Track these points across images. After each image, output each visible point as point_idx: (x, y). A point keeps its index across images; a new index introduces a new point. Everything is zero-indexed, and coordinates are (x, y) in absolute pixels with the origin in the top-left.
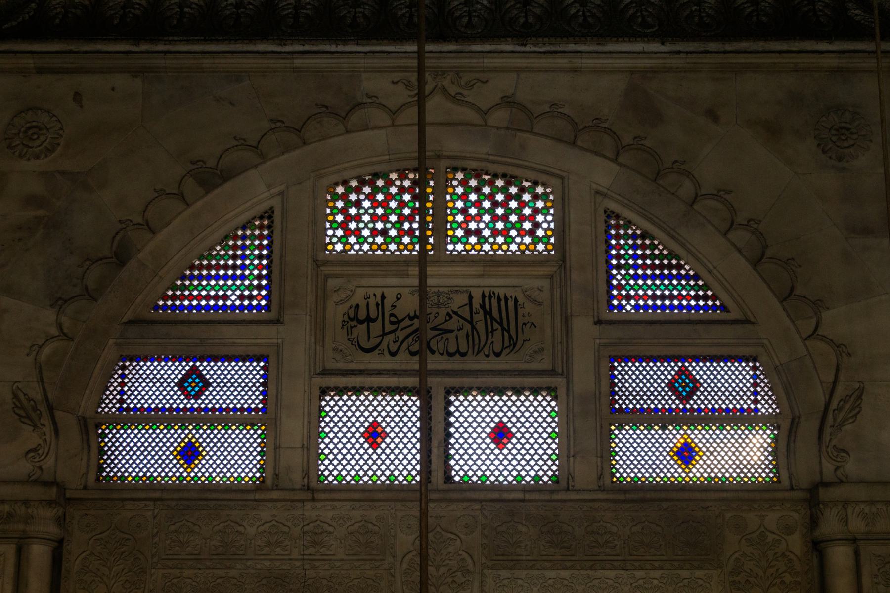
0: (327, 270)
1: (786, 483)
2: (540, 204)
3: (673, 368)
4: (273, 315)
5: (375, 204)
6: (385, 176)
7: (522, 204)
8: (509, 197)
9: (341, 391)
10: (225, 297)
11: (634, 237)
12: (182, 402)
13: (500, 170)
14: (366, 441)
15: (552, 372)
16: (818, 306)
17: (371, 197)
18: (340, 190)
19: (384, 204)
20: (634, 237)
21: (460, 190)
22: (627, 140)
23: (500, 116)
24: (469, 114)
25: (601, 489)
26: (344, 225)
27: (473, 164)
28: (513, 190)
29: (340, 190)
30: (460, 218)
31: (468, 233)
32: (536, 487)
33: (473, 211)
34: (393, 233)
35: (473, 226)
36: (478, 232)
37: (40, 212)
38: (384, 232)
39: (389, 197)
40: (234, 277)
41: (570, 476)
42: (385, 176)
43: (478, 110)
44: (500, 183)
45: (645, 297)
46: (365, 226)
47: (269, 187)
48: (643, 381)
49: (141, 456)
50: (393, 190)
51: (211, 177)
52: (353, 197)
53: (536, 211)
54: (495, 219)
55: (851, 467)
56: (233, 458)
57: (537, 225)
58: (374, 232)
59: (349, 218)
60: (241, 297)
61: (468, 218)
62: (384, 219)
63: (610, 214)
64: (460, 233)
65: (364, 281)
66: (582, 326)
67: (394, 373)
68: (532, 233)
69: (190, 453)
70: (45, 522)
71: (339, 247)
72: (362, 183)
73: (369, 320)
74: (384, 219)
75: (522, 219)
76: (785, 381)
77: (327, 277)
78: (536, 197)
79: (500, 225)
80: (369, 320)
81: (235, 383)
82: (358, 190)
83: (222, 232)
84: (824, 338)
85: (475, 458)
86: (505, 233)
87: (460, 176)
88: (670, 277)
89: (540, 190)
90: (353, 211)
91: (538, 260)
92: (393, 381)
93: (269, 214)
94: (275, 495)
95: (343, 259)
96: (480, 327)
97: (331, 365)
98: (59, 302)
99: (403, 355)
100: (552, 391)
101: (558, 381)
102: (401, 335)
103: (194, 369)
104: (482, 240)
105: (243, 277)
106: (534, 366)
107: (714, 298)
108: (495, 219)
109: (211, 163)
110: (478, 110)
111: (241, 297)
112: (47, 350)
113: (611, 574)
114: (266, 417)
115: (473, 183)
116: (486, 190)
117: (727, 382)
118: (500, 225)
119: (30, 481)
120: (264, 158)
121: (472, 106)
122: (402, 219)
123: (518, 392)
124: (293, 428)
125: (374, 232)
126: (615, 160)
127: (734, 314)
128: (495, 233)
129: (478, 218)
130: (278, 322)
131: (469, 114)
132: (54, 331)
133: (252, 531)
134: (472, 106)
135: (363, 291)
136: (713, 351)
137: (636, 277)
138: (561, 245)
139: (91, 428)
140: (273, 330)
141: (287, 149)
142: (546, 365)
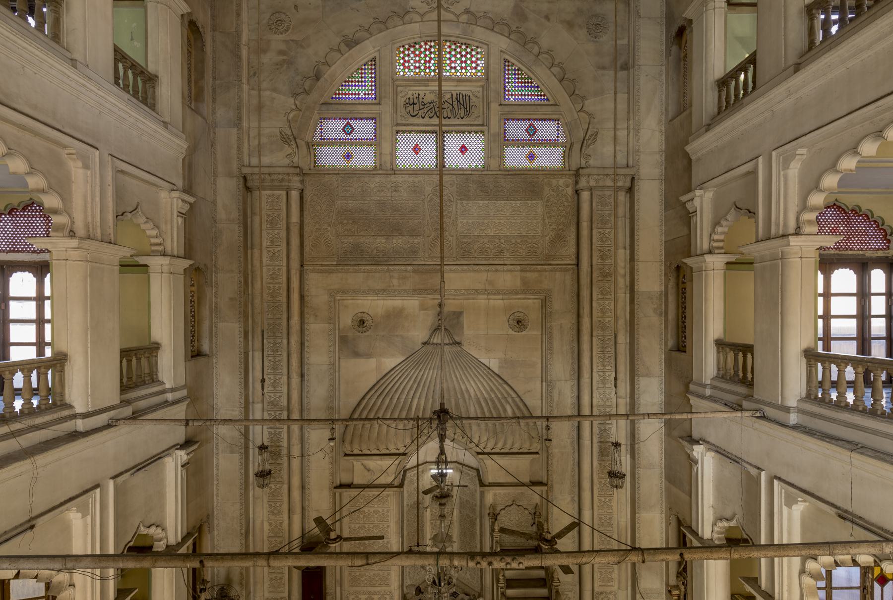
0: (397, 83)
1: (567, 168)
2: (479, 56)
3: (528, 123)
4: (377, 101)
5: (416, 56)
6: (419, 43)
7: (472, 56)
8: (467, 53)
9: (404, 132)
10: (359, 94)
11: (515, 70)
12: (344, 136)
13: (464, 41)
14: (415, 152)
15: (483, 125)
16: (583, 98)
17: (413, 52)
18: (402, 49)
19: (419, 56)
20: (515, 70)
21: (448, 50)
22: (514, 28)
23: (464, 18)
24: (452, 17)
25: (500, 170)
26: (403, 64)
27: (453, 39)
28: (469, 50)
29: (402, 49)
30: (448, 62)
31: (451, 68)
32: (476, 169)
33: (453, 59)
34: (422, 68)
35: (453, 65)
36: (455, 68)
37: (285, 57)
38: (419, 67)
39: (421, 53)
40: (362, 86)
41: (489, 165)
42: (419, 43)
43: (456, 15)
44: (464, 47)
45: (518, 95)
46: (412, 67)
47: (374, 48)
48: (517, 129)
49: (331, 158)
50: (422, 50)
51: (352, 43)
52: (407, 52)
53: (477, 59)
54: (462, 62)
55: (592, 162)
56: (364, 159)
57: (478, 65)
58: (415, 67)
59: (405, 61)
60: (365, 94)
61: (452, 62)
62: (419, 62)
63: (506, 61)
64: (448, 68)
65: (412, 88)
66: (494, 106)
67: (424, 125)
68: (476, 68)
69: (348, 156)
70: (296, 182)
71: (402, 74)
72: (410, 46)
73: (414, 104)
74: (419, 62)
75: (472, 62)
76: (570, 129)
77: (398, 86)
78: (477, 53)
79: (463, 65)
80: (414, 104)
81: (364, 129)
82: (409, 49)
83: (356, 67)
84: (585, 112)
85: (454, 159)
86: (465, 68)
87: (448, 44)
88: (528, 87)
89: (479, 50)
90: (407, 58)
91: (477, 80)
92: (423, 128)
93: (374, 59)
94: (380, 172)
95: (404, 79)
96: (456, 107)
97: (400, 122)
98: (295, 95)
99: (427, 118)
100: (482, 132)
101: (485, 128)
102: (426, 110)
103: (348, 123)
104: (457, 71)
105: (365, 86)
106: (476, 123)
107: (544, 95)
108: (462, 62)
109: (351, 37)
110: (456, 15)
111: (365, 94)
112: (291, 115)
113: (503, 202)
114: (376, 142)
115: (453, 47)
116: (458, 50)
117: (547, 130)
118: (463, 65)
119: (288, 166)
120: (371, 35)
121: (453, 13)
122: (426, 62)
123: (470, 133)
124: (386, 147)
125: (415, 67)
126: (508, 37)
127: (551, 103)
128: (462, 68)
129: (455, 62)
130: (379, 104)
131: (452, 17)
132: (294, 107)
133: (372, 186)
134: (453, 13)
135: (412, 92)
136: (543, 117)
137: (515, 87)
138: (487, 74)
139: (310, 146)
140: (377, 107)
141: (381, 31)
142: (480, 122)
